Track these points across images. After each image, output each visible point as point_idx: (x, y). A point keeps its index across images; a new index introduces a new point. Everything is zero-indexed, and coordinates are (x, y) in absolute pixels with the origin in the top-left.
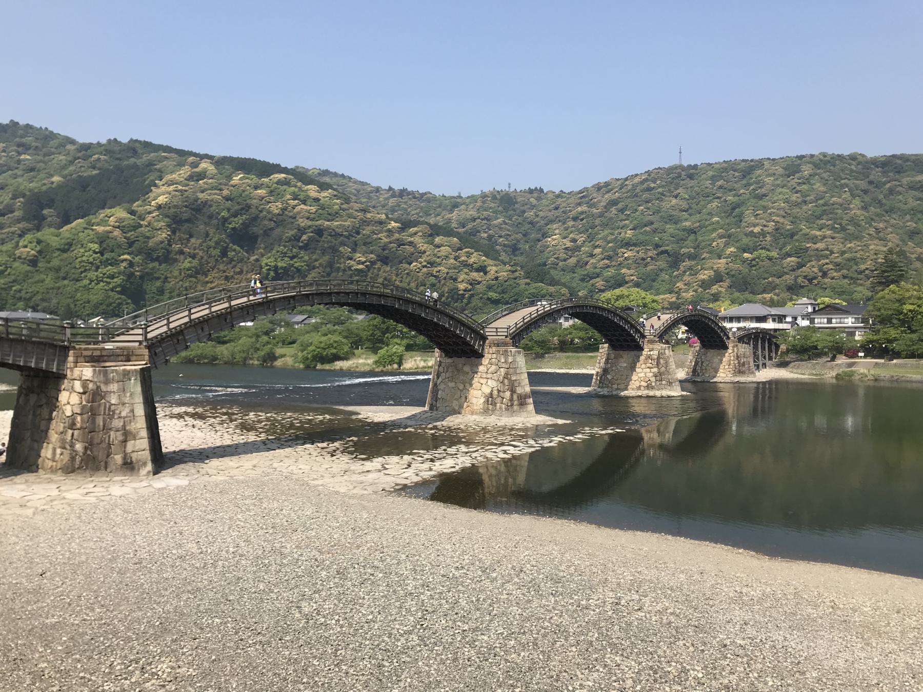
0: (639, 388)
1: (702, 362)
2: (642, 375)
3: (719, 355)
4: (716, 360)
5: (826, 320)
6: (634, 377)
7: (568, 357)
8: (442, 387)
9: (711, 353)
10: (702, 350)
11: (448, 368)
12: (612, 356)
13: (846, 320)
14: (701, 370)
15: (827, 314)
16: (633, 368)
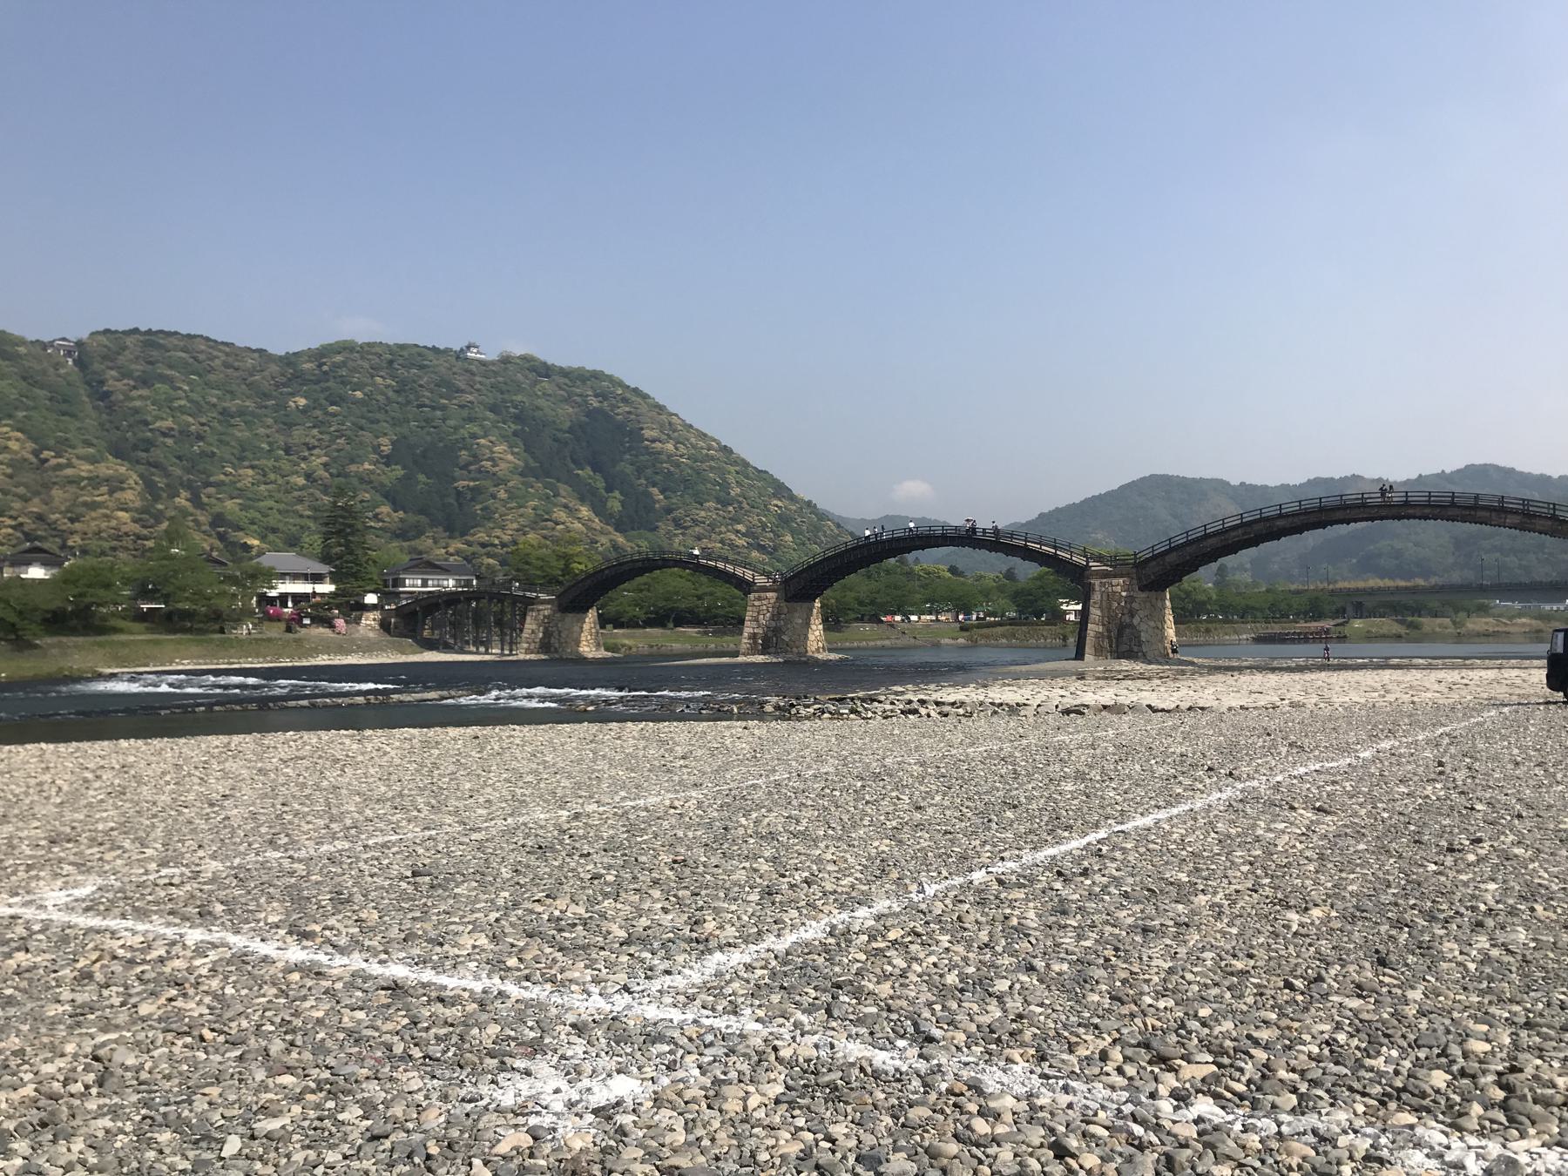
0: (818, 650)
1: (560, 632)
2: (817, 633)
3: (578, 621)
4: (576, 629)
5: (419, 582)
6: (811, 637)
7: (101, 645)
8: (1143, 627)
9: (570, 617)
10: (558, 615)
11: (1145, 602)
12: (786, 610)
13: (445, 583)
14: (560, 643)
15: (423, 573)
16: (807, 624)
